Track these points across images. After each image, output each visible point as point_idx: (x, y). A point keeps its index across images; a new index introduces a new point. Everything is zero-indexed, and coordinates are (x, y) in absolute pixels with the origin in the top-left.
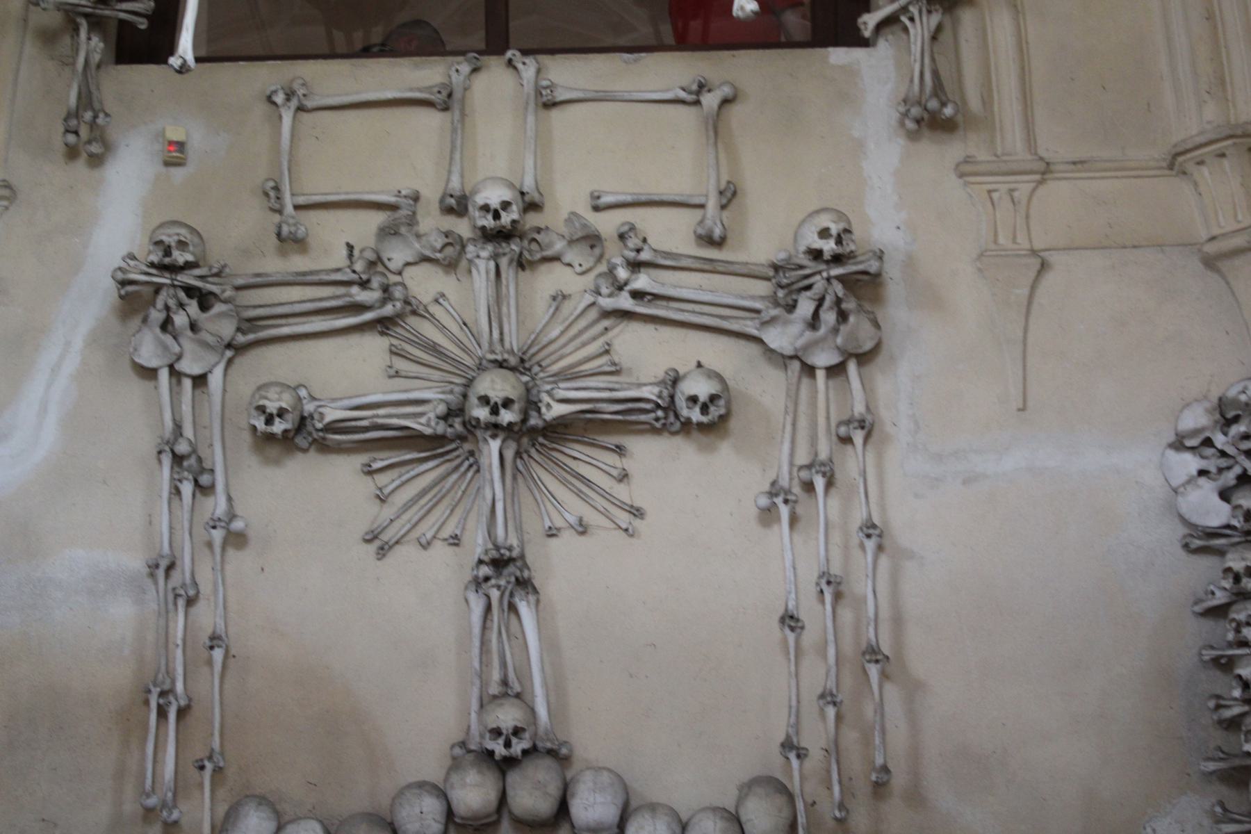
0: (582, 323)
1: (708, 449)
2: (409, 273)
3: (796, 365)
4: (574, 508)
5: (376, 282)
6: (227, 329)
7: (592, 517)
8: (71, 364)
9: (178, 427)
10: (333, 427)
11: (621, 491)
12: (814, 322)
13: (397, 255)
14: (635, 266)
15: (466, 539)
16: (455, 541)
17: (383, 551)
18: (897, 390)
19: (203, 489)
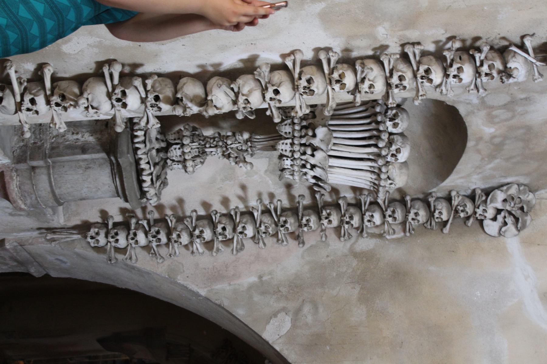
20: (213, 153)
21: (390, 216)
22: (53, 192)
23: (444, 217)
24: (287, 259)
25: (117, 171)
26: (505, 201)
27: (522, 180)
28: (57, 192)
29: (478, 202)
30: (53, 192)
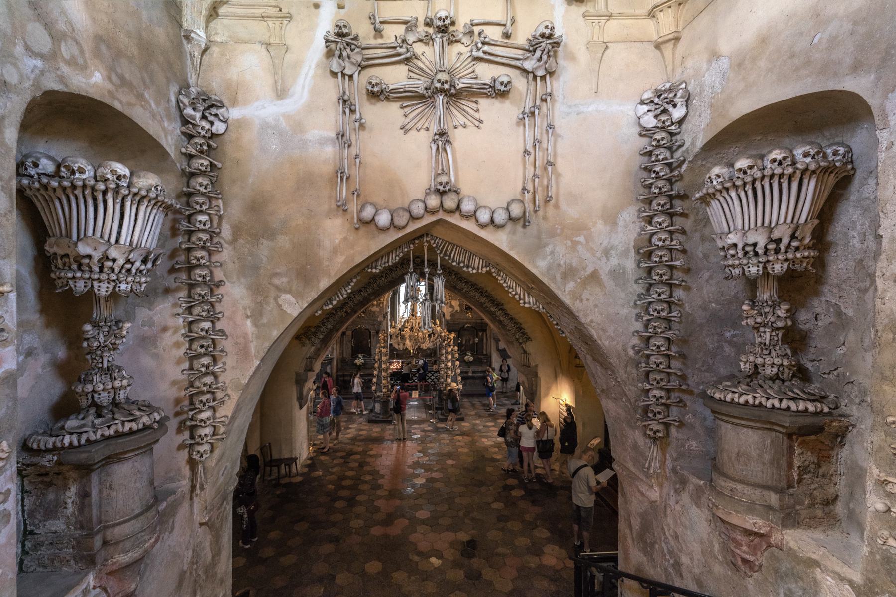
0: (466, 62)
1: (503, 102)
2: (414, 45)
3: (531, 75)
4: (462, 120)
5: (405, 46)
6: (359, 58)
7: (468, 123)
8: (311, 73)
9: (344, 93)
10: (393, 91)
11: (476, 115)
12: (540, 59)
13: (411, 38)
14: (484, 43)
15: (430, 129)
16: (427, 129)
17: (406, 132)
18: (558, 86)
19: (352, 112)
20: (110, 359)
21: (201, 207)
22: (137, 517)
23: (206, 163)
24: (235, 294)
25: (112, 459)
26: (194, 109)
27: (174, 89)
28: (137, 512)
29: (194, 132)
30: (137, 517)
